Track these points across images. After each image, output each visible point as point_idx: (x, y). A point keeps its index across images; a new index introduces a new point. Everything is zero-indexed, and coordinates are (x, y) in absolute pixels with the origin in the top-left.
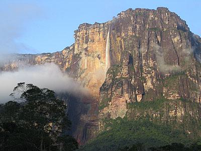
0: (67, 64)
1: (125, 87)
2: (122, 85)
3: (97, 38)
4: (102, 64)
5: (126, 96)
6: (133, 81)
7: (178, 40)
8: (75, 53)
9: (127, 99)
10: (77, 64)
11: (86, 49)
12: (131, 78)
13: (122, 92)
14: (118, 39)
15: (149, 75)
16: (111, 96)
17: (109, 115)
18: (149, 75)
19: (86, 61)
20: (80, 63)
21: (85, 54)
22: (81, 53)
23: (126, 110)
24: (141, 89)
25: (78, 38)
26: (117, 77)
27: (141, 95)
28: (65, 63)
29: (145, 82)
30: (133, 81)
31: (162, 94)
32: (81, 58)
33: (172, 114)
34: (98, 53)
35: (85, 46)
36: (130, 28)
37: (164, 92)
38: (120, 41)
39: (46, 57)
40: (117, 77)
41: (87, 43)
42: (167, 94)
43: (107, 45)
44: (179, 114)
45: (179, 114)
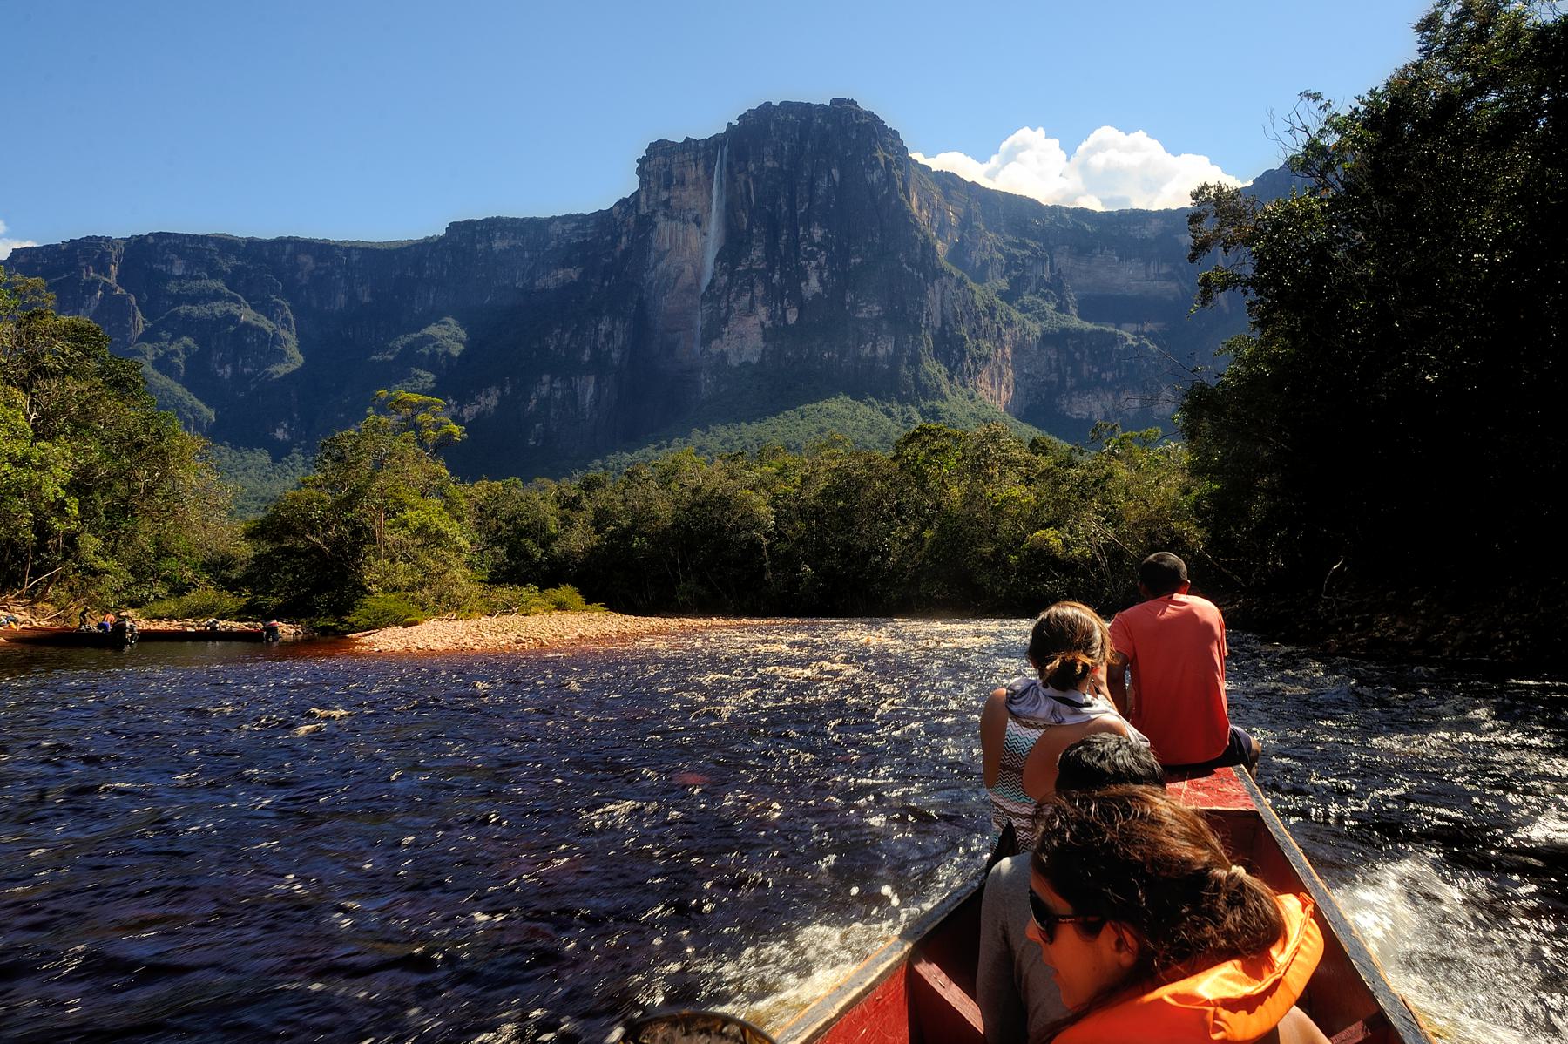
0: (624, 239)
1: (759, 290)
2: (752, 286)
5: (762, 311)
7: (879, 179)
9: (764, 318)
11: (666, 204)
13: (752, 304)
14: (742, 177)
15: (814, 263)
17: (723, 356)
18: (814, 263)
19: (667, 233)
21: (665, 215)
22: (654, 212)
23: (762, 345)
28: (620, 236)
29: (806, 279)
31: (844, 305)
32: (655, 225)
33: (866, 350)
35: (664, 195)
36: (768, 150)
41: (667, 188)
42: (854, 307)
43: (715, 194)
44: (881, 352)
45: (881, 352)
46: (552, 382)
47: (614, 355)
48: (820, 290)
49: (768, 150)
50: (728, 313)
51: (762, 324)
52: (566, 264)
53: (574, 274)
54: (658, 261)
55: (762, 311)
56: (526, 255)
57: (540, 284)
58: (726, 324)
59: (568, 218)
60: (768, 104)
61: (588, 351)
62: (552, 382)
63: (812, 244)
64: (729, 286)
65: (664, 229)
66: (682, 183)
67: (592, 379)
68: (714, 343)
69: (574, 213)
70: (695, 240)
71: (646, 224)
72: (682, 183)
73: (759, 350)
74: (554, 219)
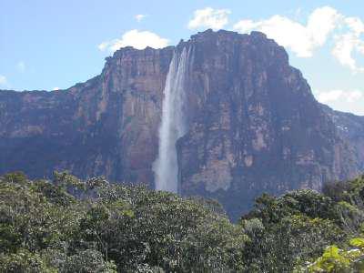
0: (80, 109)
1: (228, 143)
5: (230, 157)
6: (238, 135)
11: (132, 86)
12: (235, 132)
13: (223, 152)
15: (260, 128)
16: (204, 157)
17: (203, 185)
18: (260, 128)
20: (124, 106)
21: (132, 93)
22: (124, 91)
23: (230, 178)
24: (250, 148)
25: (118, 68)
26: (214, 128)
27: (251, 157)
29: (256, 138)
30: (238, 135)
32: (125, 99)
34: (154, 93)
35: (131, 81)
36: (217, 58)
37: (286, 153)
38: (199, 77)
39: (40, 98)
40: (214, 128)
41: (134, 75)
48: (265, 145)
49: (217, 58)
50: (206, 155)
51: (230, 164)
53: (39, 129)
55: (230, 157)
57: (14, 134)
58: (204, 163)
59: (35, 93)
60: (210, 30)
63: (258, 116)
64: (206, 139)
65: (131, 103)
66: (144, 74)
68: (195, 176)
69: (40, 89)
70: (151, 113)
71: (117, 99)
72: (144, 74)
73: (229, 182)
74: (25, 92)
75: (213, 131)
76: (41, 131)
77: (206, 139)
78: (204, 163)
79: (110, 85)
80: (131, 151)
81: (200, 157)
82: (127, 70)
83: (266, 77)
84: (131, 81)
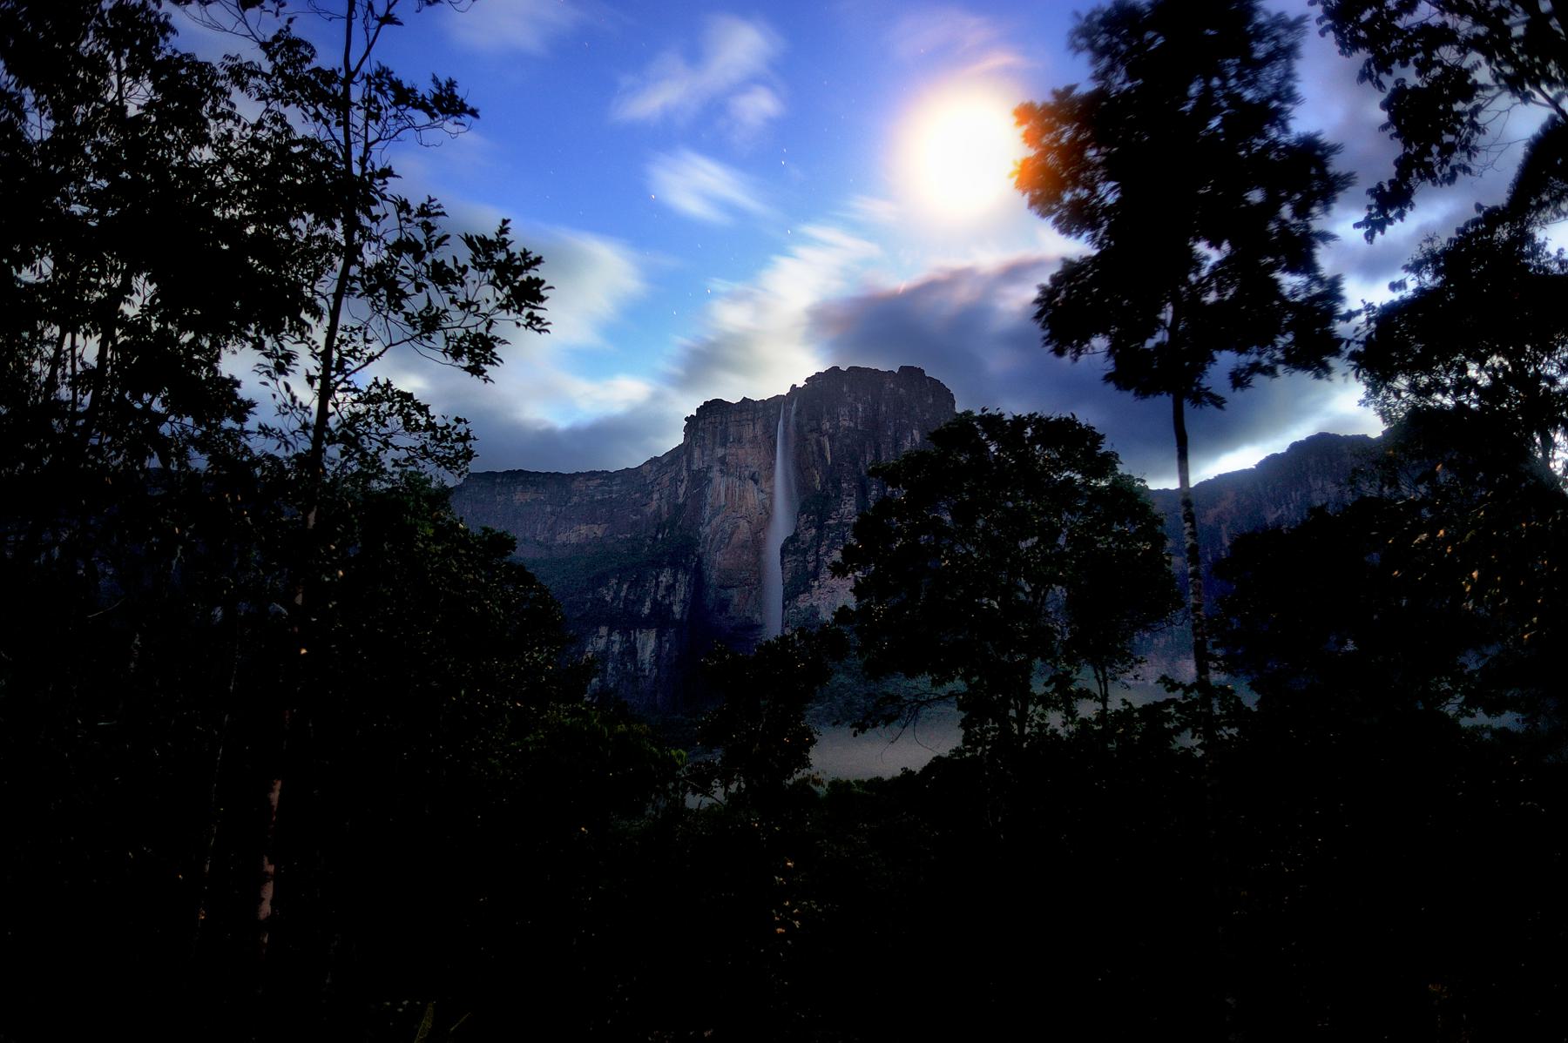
0: (656, 496)
3: (748, 433)
4: (762, 496)
8: (695, 467)
10: (701, 495)
11: (722, 461)
14: (815, 435)
16: (817, 567)
20: (709, 492)
22: (709, 468)
32: (710, 481)
35: (720, 452)
36: (843, 410)
41: (724, 445)
46: (609, 635)
47: (677, 609)
49: (843, 410)
50: (817, 567)
52: (592, 519)
53: (598, 531)
54: (714, 515)
56: (549, 509)
57: (561, 539)
58: (816, 577)
61: (648, 604)
62: (609, 635)
64: (818, 539)
65: (719, 484)
67: (653, 634)
68: (802, 597)
72: (739, 440)
75: (829, 526)
76: (599, 534)
77: (818, 539)
78: (816, 577)
79: (689, 462)
80: (719, 561)
81: (811, 567)
82: (714, 436)
83: (918, 439)
84: (720, 452)
